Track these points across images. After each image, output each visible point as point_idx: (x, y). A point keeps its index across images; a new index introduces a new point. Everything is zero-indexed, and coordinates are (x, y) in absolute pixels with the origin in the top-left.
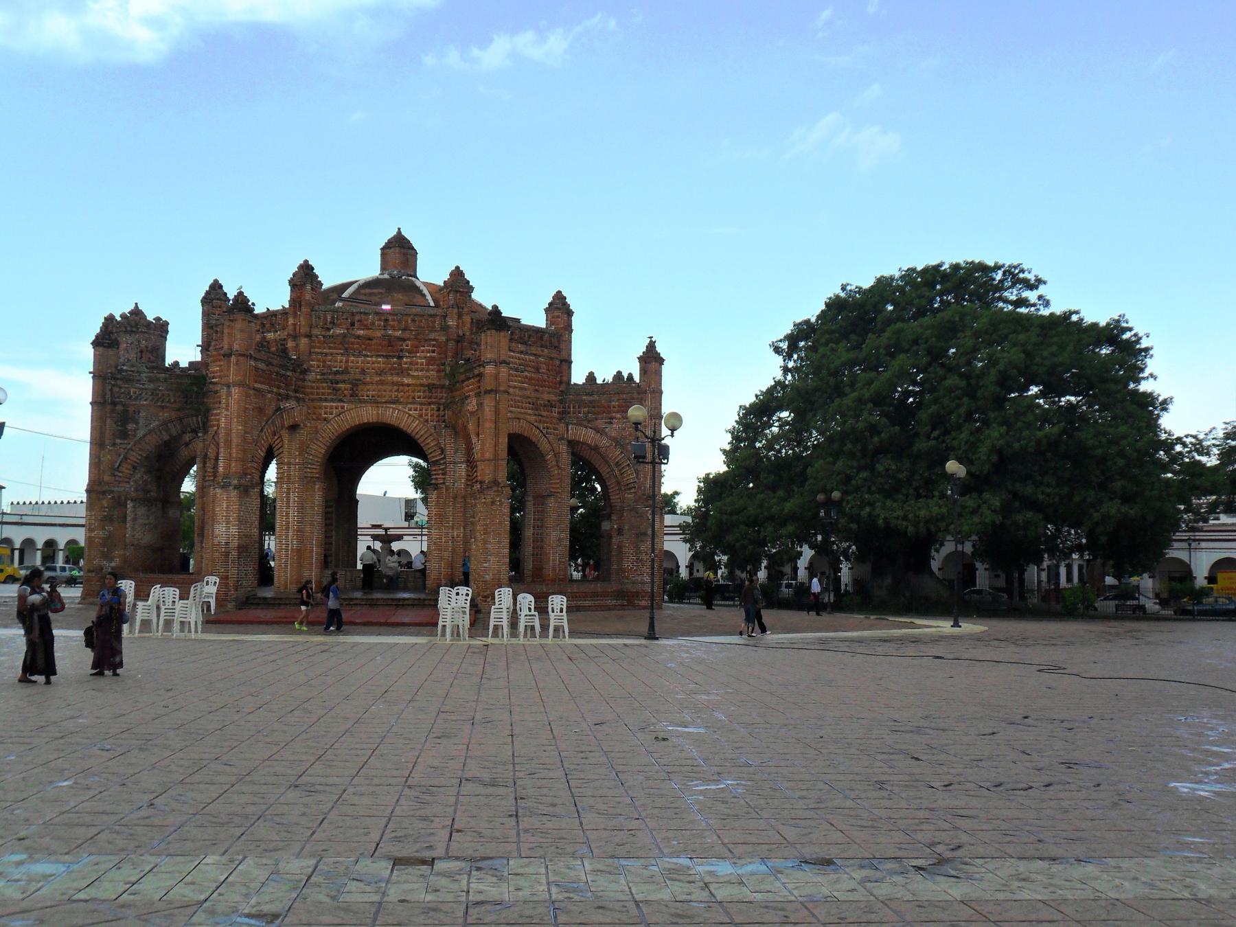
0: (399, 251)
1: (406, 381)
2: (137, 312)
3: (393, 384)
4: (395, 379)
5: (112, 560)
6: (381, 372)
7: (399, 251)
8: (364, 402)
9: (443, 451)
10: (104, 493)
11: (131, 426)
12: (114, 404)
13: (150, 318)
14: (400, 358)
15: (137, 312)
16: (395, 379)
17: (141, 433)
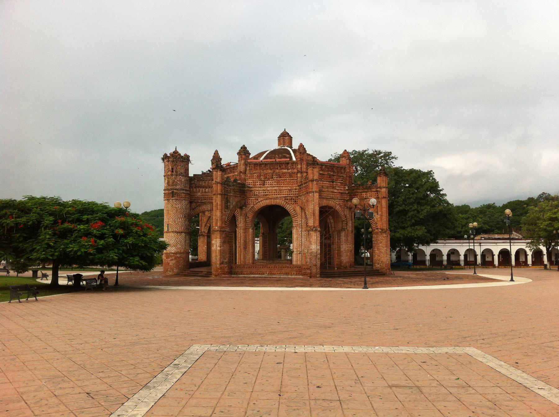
0: (285, 137)
1: (336, 191)
2: (176, 152)
3: (332, 192)
4: (332, 190)
5: (225, 259)
6: (328, 187)
7: (285, 137)
8: (323, 198)
9: (346, 217)
10: (223, 231)
11: (229, 204)
12: (225, 195)
13: (182, 154)
14: (333, 182)
15: (176, 152)
16: (332, 190)
17: (231, 206)
